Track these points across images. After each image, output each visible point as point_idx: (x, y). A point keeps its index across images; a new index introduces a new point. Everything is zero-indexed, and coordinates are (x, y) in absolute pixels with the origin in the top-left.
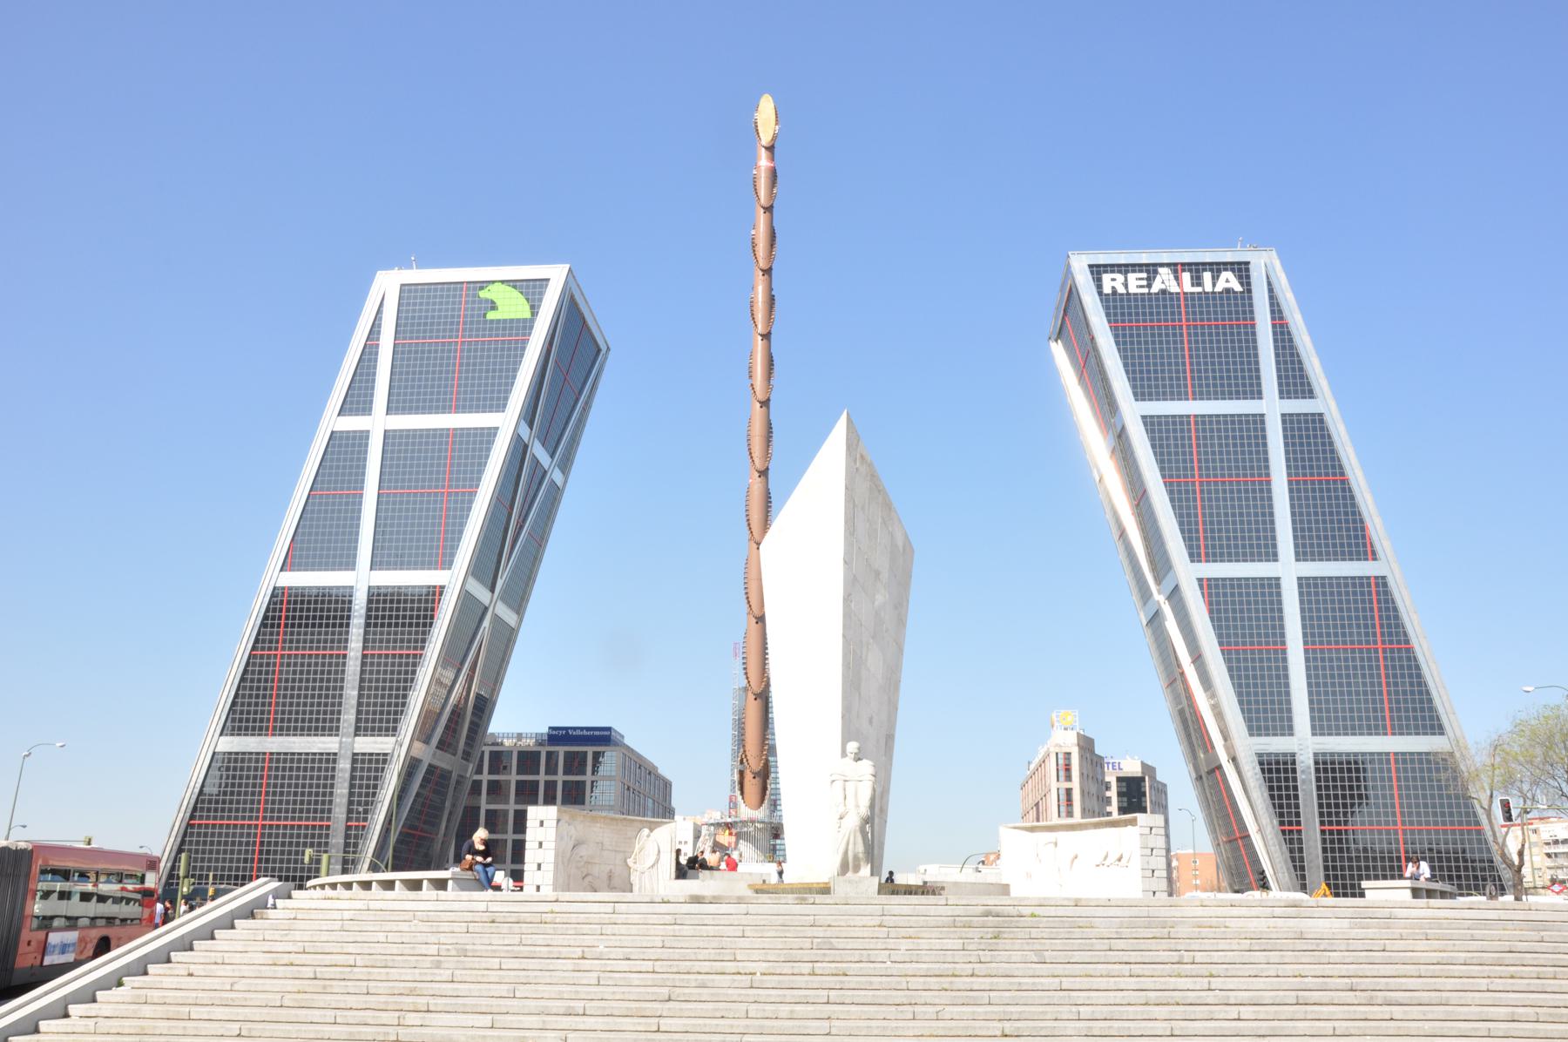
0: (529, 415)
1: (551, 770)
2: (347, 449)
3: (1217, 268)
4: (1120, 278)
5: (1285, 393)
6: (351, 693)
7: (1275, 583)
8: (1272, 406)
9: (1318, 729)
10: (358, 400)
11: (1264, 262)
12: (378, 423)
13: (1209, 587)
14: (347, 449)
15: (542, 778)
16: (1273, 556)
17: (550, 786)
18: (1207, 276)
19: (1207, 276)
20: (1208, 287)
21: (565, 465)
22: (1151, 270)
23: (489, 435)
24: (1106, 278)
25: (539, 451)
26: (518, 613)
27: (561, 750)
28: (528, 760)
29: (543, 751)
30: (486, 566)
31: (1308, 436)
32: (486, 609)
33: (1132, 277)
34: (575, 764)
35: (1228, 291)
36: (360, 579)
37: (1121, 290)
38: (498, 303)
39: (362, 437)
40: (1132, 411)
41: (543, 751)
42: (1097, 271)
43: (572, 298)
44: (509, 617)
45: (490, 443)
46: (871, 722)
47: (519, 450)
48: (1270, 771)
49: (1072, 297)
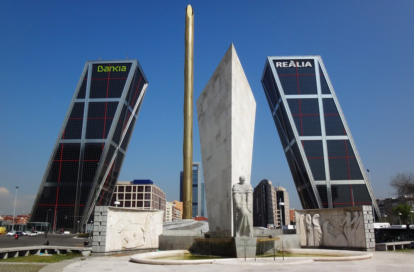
0: (127, 99)
1: (134, 191)
3: (305, 61)
4: (281, 63)
5: (323, 92)
7: (321, 141)
8: (320, 96)
9: (332, 178)
11: (317, 59)
12: (87, 100)
13: (303, 142)
15: (132, 193)
17: (134, 195)
18: (303, 63)
19: (303, 63)
20: (303, 65)
22: (289, 61)
23: (116, 104)
24: (277, 63)
25: (130, 108)
27: (137, 186)
28: (129, 189)
29: (132, 186)
30: (116, 138)
31: (329, 104)
33: (284, 63)
34: (140, 189)
35: (308, 67)
36: (83, 141)
37: (281, 66)
40: (284, 97)
41: (132, 186)
42: (275, 61)
44: (122, 151)
45: (117, 106)
47: (125, 107)
48: (320, 189)
49: (268, 68)
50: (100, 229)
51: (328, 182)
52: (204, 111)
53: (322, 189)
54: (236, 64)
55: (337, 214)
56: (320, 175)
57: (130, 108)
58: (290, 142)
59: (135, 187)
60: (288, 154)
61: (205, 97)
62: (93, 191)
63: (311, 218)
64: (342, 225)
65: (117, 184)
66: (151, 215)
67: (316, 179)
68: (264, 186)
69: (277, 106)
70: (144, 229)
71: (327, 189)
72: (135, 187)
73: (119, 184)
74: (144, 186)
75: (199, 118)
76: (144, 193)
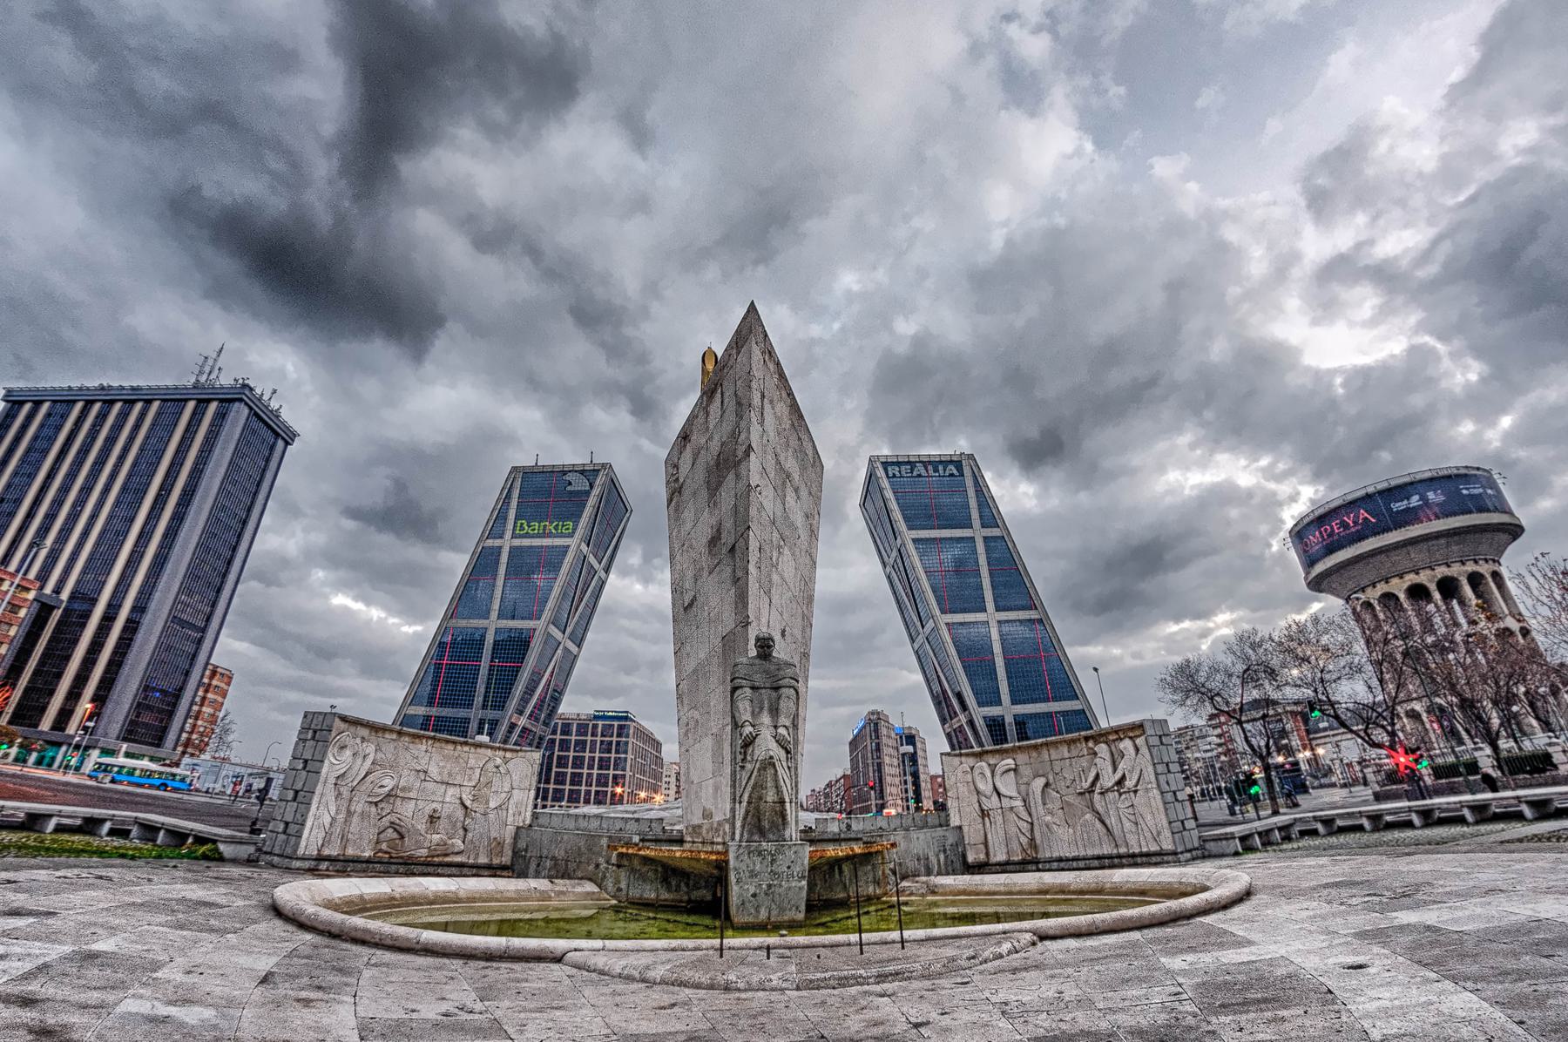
3: (945, 463)
6: (481, 688)
8: (978, 533)
17: (593, 743)
21: (607, 571)
25: (592, 559)
28: (582, 729)
36: (493, 626)
44: (573, 648)
46: (783, 632)
51: (1008, 710)
55: (1066, 755)
56: (989, 697)
59: (595, 727)
63: (988, 774)
69: (895, 554)
70: (468, 803)
74: (616, 723)
75: (670, 501)
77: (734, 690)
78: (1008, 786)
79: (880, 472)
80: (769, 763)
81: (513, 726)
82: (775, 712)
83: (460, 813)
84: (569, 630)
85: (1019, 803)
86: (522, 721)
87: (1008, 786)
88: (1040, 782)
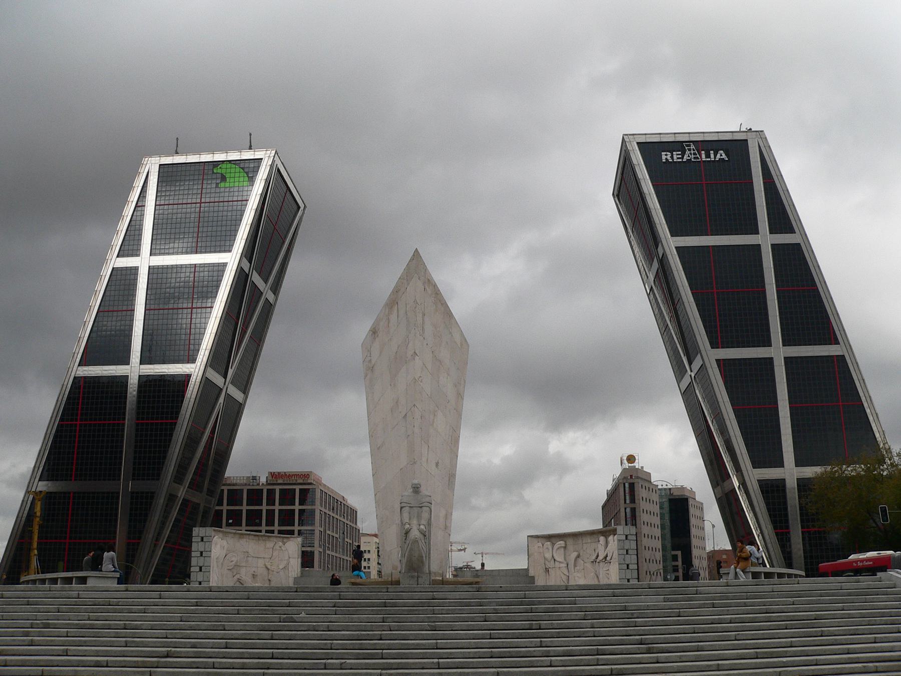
0: (248, 253)
1: (271, 501)
2: (123, 281)
8: (765, 239)
10: (130, 247)
14: (123, 281)
15: (264, 507)
16: (767, 343)
17: (270, 513)
21: (276, 289)
25: (256, 278)
26: (244, 393)
27: (277, 488)
28: (255, 496)
32: (221, 390)
36: (134, 369)
38: (227, 176)
39: (134, 271)
40: (671, 243)
43: (279, 170)
44: (238, 395)
47: (241, 277)
50: (201, 562)
51: (790, 472)
52: (373, 362)
53: (773, 491)
54: (424, 283)
56: (765, 451)
57: (256, 278)
58: (690, 363)
59: (271, 492)
60: (688, 395)
61: (375, 339)
62: (161, 501)
64: (594, 557)
65: (224, 485)
66: (281, 544)
67: (757, 463)
68: (627, 485)
69: (656, 265)
70: (269, 567)
71: (787, 491)
72: (271, 492)
73: (229, 485)
74: (297, 488)
76: (245, 508)
77: (402, 508)
78: (559, 557)
79: (637, 158)
80: (416, 541)
81: (172, 498)
82: (419, 517)
83: (265, 572)
84: (231, 372)
85: (564, 565)
86: (182, 492)
87: (559, 557)
88: (575, 554)
